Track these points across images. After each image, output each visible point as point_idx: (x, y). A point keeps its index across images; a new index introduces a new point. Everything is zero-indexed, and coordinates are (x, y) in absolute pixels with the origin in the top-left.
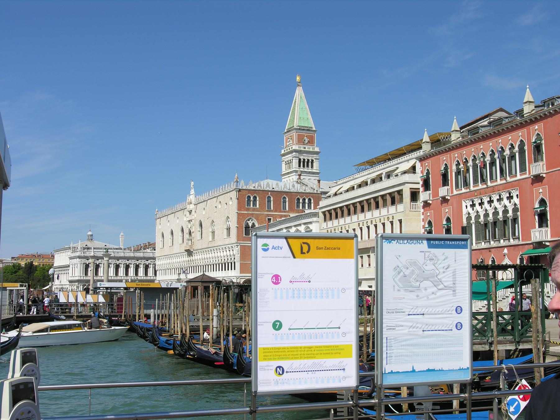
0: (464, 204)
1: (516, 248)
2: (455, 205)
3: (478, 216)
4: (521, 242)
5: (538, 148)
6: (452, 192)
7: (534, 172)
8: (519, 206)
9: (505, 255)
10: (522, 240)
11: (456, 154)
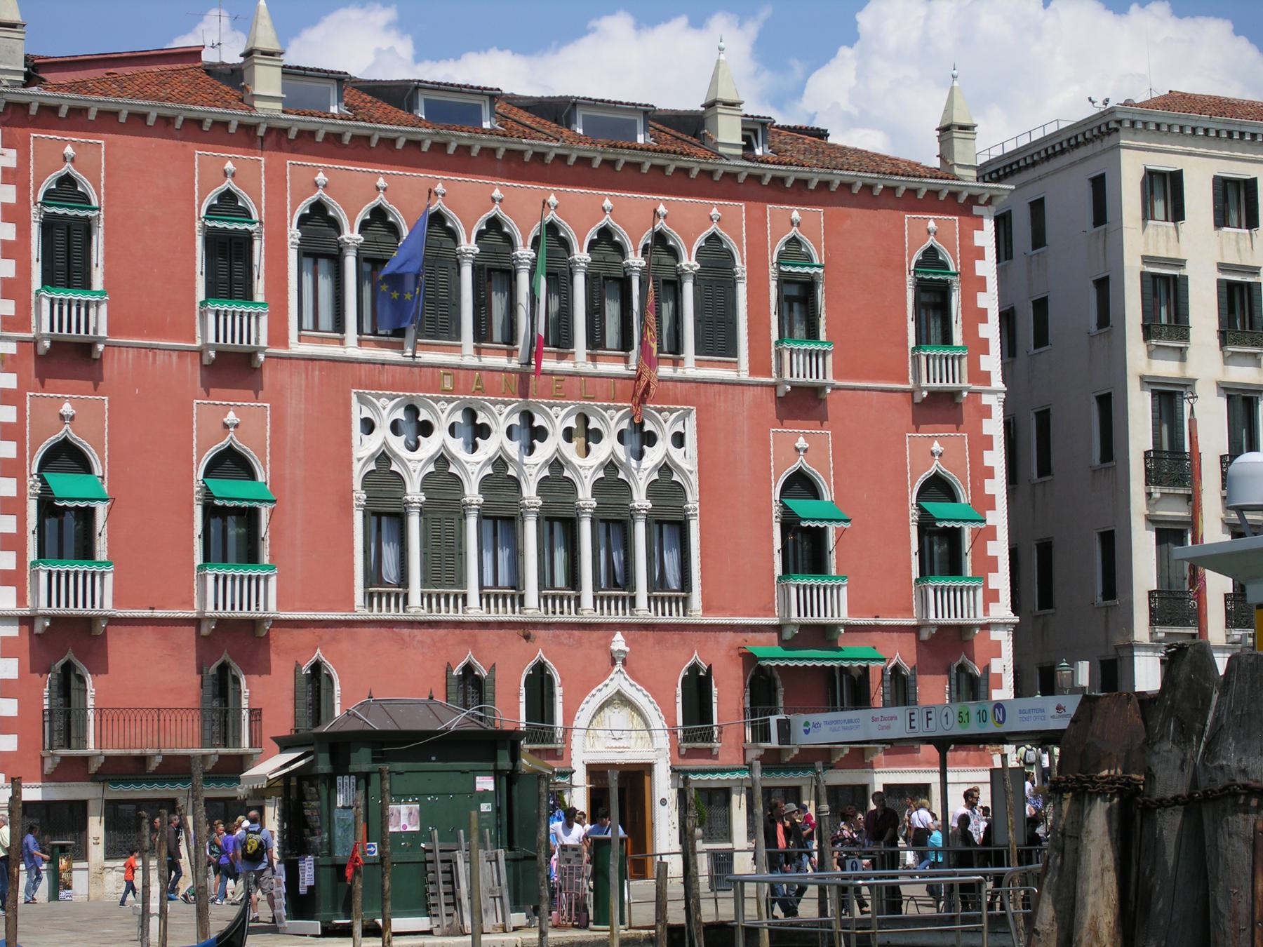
0: (358, 413)
1: (676, 636)
2: (295, 405)
4: (697, 614)
6: (278, 335)
8: (694, 479)
9: (614, 663)
10: (706, 609)
11: (321, 177)
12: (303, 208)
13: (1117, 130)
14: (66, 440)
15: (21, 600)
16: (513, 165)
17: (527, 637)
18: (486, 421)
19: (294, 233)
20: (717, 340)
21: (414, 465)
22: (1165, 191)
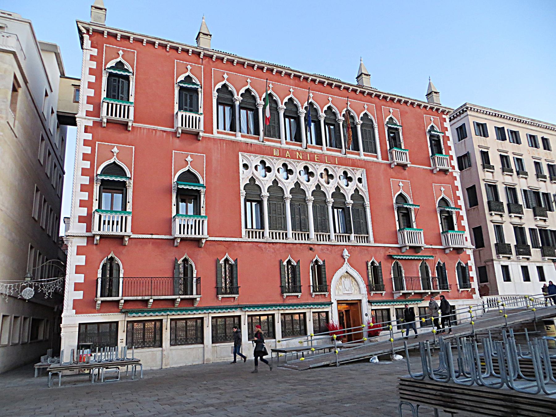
2: (216, 156)
6: (209, 129)
10: (375, 241)
12: (219, 86)
13: (466, 111)
14: (114, 162)
15: (89, 229)
16: (297, 81)
17: (311, 249)
18: (291, 168)
19: (215, 94)
20: (370, 148)
22: (482, 129)
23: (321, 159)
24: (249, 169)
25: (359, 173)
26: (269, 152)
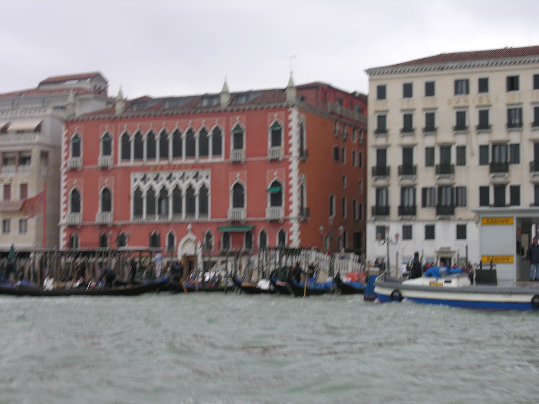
3: (151, 191)
4: (209, 218)
5: (238, 138)
6: (116, 162)
7: (232, 158)
20: (217, 152)
21: (144, 188)
23: (180, 167)
24: (135, 181)
25: (203, 173)
26: (148, 168)
